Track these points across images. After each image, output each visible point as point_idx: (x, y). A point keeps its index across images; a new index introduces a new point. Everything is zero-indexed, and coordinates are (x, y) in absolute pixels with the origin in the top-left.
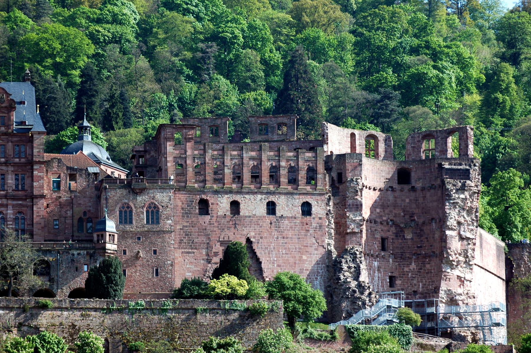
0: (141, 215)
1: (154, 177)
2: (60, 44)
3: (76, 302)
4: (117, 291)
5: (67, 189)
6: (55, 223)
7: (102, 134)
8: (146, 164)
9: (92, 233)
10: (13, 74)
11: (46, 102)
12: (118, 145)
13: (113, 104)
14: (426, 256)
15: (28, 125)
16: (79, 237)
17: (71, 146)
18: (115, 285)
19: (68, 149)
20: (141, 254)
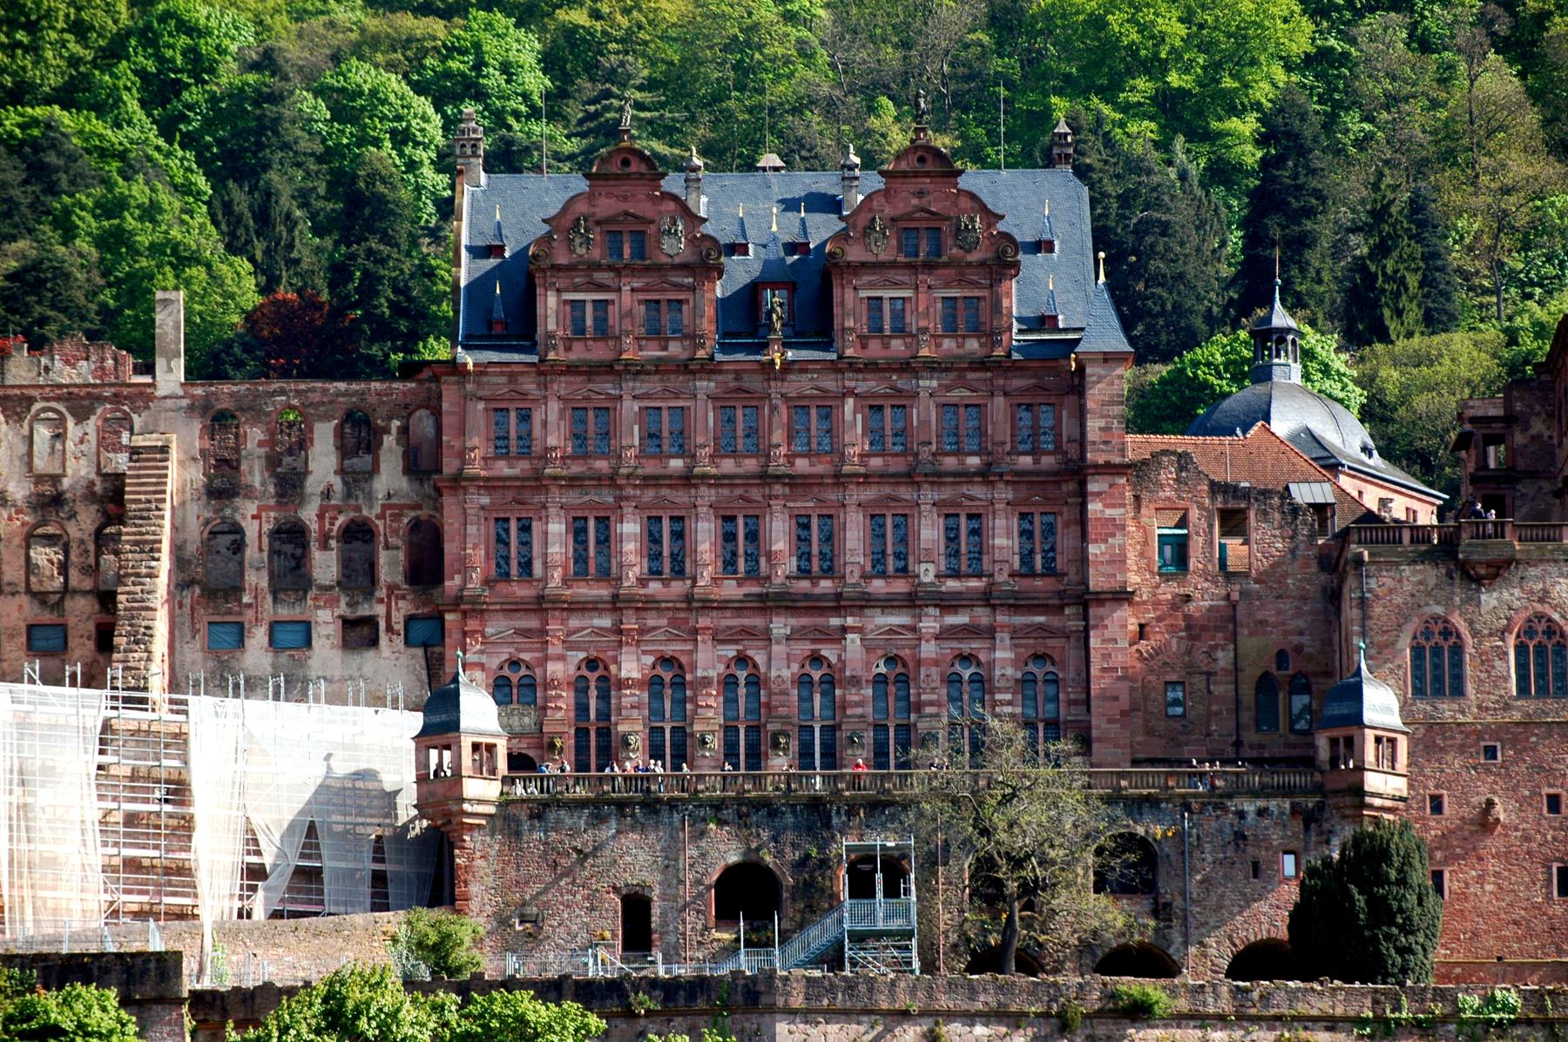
0: (1497, 663)
1: (1543, 515)
2: (1180, 20)
3: (1255, 995)
4: (1410, 950)
5: (1214, 567)
6: (1171, 695)
7: (1344, 356)
8: (1512, 468)
9: (1308, 733)
10: (1009, 137)
11: (1130, 239)
12: (1404, 399)
13: (1383, 240)
15: (1066, 330)
16: (1261, 746)
17: (1226, 404)
18: (1401, 928)
19: (1217, 415)
20: (1500, 812)
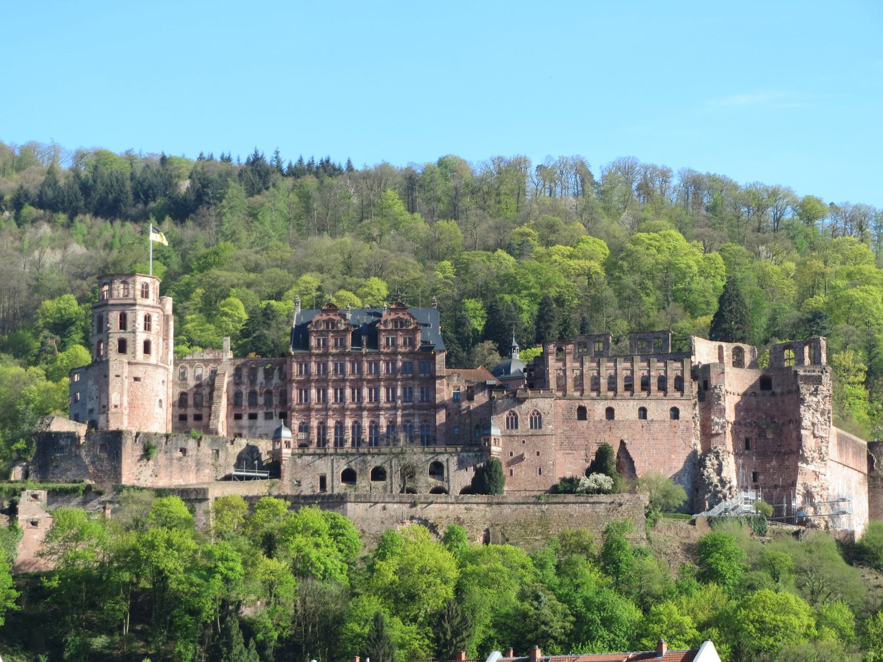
14: (785, 454)
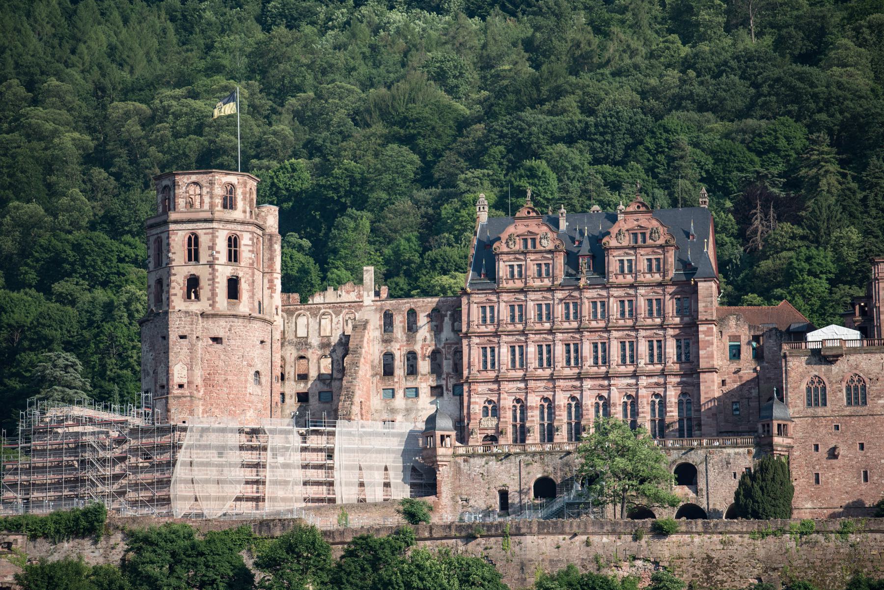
6: (735, 407)
